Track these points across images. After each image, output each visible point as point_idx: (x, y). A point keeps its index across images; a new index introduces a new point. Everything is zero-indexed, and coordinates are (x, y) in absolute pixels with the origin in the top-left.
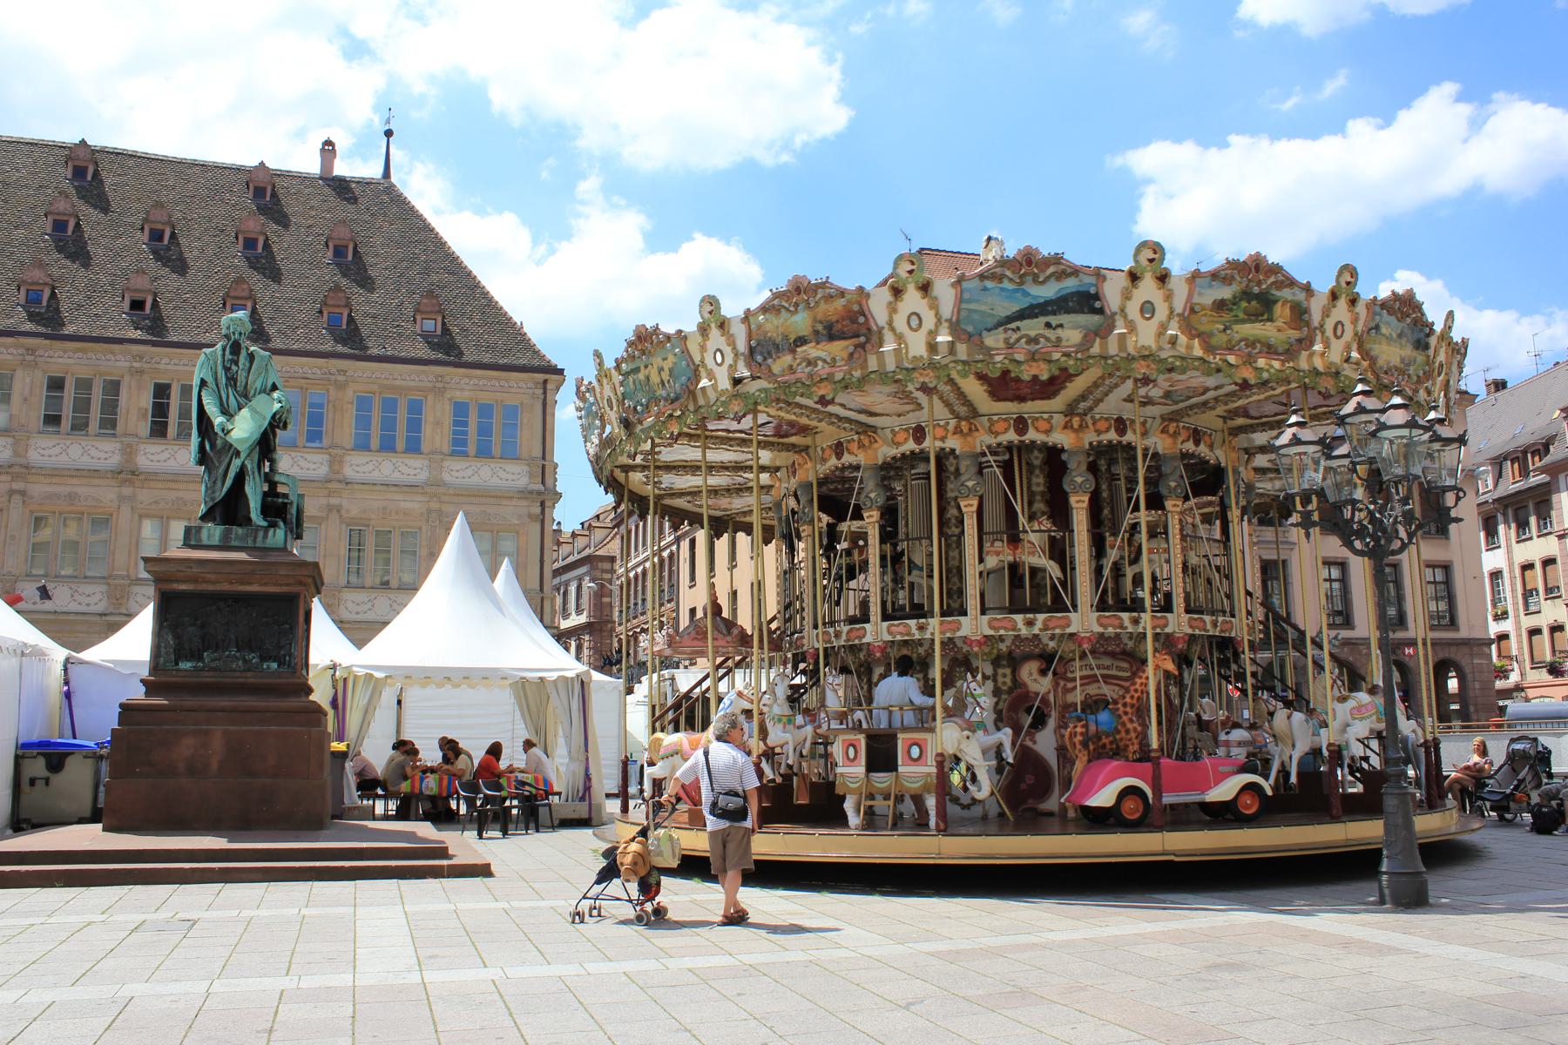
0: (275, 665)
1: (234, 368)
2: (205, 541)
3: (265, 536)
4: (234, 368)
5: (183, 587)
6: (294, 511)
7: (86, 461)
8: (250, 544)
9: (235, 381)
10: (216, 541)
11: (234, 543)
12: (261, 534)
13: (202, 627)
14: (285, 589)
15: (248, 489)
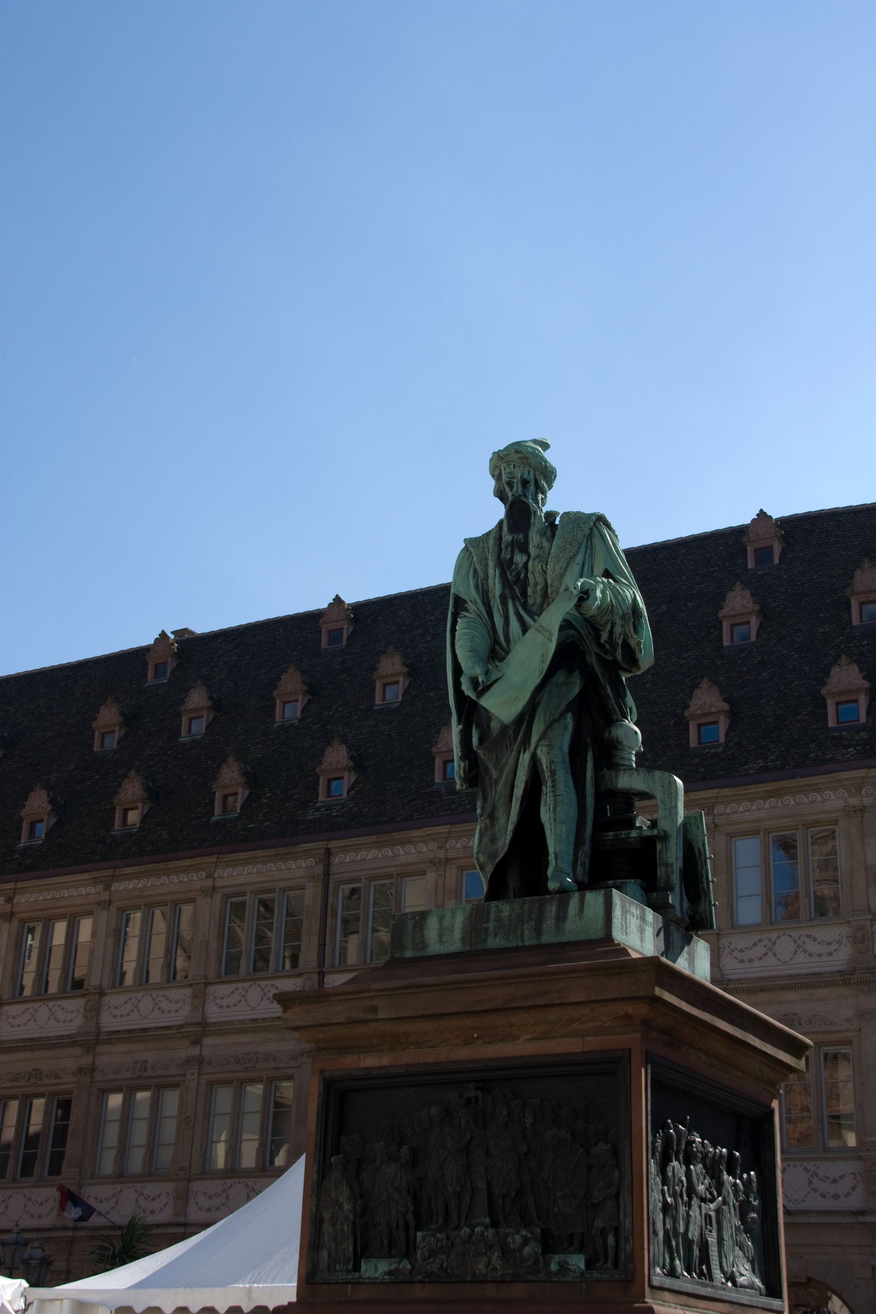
0: (578, 1262)
1: (520, 559)
2: (434, 947)
3: (562, 916)
4: (520, 559)
5: (370, 1061)
6: (673, 855)
7: (802, 964)
8: (529, 940)
9: (523, 584)
10: (455, 943)
11: (494, 942)
12: (552, 910)
13: (414, 1162)
14: (592, 1043)
15: (545, 815)
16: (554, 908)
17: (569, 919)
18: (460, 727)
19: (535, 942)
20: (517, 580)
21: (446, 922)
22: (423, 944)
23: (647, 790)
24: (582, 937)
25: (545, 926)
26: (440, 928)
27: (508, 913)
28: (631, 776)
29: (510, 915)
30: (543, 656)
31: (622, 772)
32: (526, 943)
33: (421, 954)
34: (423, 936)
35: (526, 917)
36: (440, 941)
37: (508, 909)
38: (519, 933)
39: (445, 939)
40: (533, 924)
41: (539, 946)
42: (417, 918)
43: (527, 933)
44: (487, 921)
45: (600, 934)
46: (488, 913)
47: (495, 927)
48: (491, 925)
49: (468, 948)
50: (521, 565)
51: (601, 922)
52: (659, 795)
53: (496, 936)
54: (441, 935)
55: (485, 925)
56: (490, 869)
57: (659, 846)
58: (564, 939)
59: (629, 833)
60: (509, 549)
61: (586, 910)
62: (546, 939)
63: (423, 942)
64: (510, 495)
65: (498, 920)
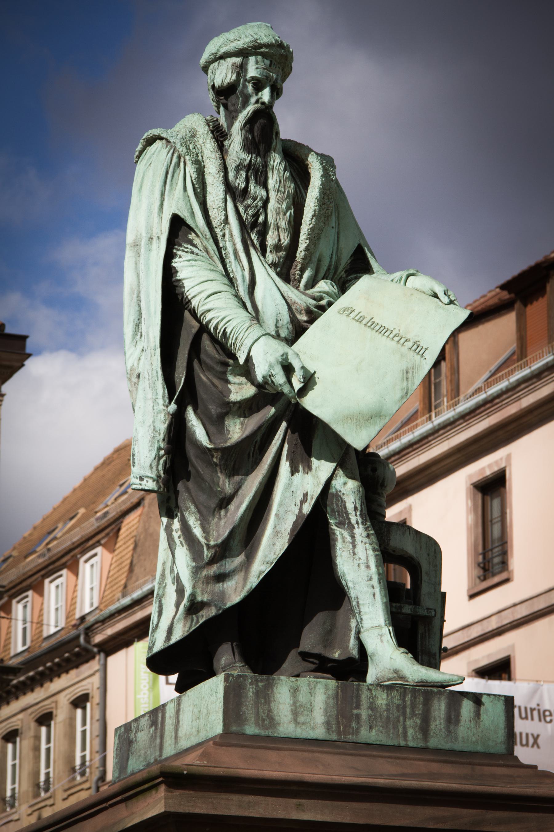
2: (286, 727)
3: (453, 718)
8: (413, 738)
10: (316, 725)
11: (367, 735)
12: (440, 708)
16: (443, 706)
17: (462, 723)
18: (173, 407)
19: (421, 744)
20: (254, 224)
21: (302, 697)
22: (270, 720)
23: (415, 556)
24: (480, 748)
25: (433, 726)
26: (294, 704)
27: (384, 702)
28: (404, 534)
29: (387, 705)
30: (407, 374)
31: (394, 527)
32: (411, 744)
33: (269, 733)
34: (270, 711)
35: (408, 710)
36: (295, 721)
37: (384, 696)
38: (401, 730)
39: (301, 719)
40: (419, 721)
41: (425, 750)
42: (260, 684)
43: (410, 732)
44: (358, 707)
45: (501, 749)
46: (358, 697)
47: (370, 716)
48: (364, 713)
49: (334, 737)
50: (260, 204)
51: (501, 734)
52: (425, 566)
53: (371, 728)
54: (295, 714)
55: (355, 712)
56: (212, 612)
57: (421, 629)
58: (458, 747)
59: (401, 608)
60: (243, 174)
61: (483, 716)
62: (433, 743)
63: (271, 719)
64: (253, 100)
65: (372, 707)
